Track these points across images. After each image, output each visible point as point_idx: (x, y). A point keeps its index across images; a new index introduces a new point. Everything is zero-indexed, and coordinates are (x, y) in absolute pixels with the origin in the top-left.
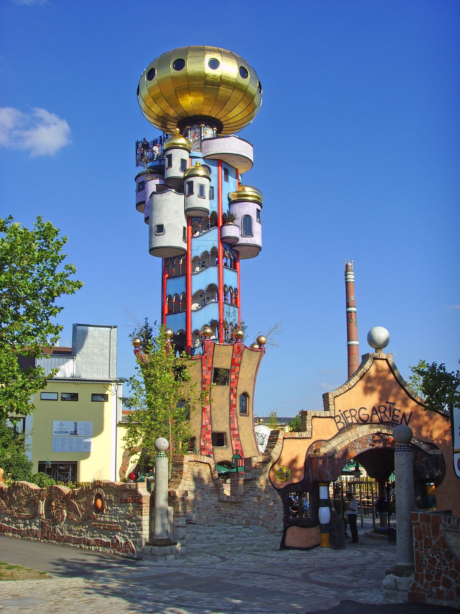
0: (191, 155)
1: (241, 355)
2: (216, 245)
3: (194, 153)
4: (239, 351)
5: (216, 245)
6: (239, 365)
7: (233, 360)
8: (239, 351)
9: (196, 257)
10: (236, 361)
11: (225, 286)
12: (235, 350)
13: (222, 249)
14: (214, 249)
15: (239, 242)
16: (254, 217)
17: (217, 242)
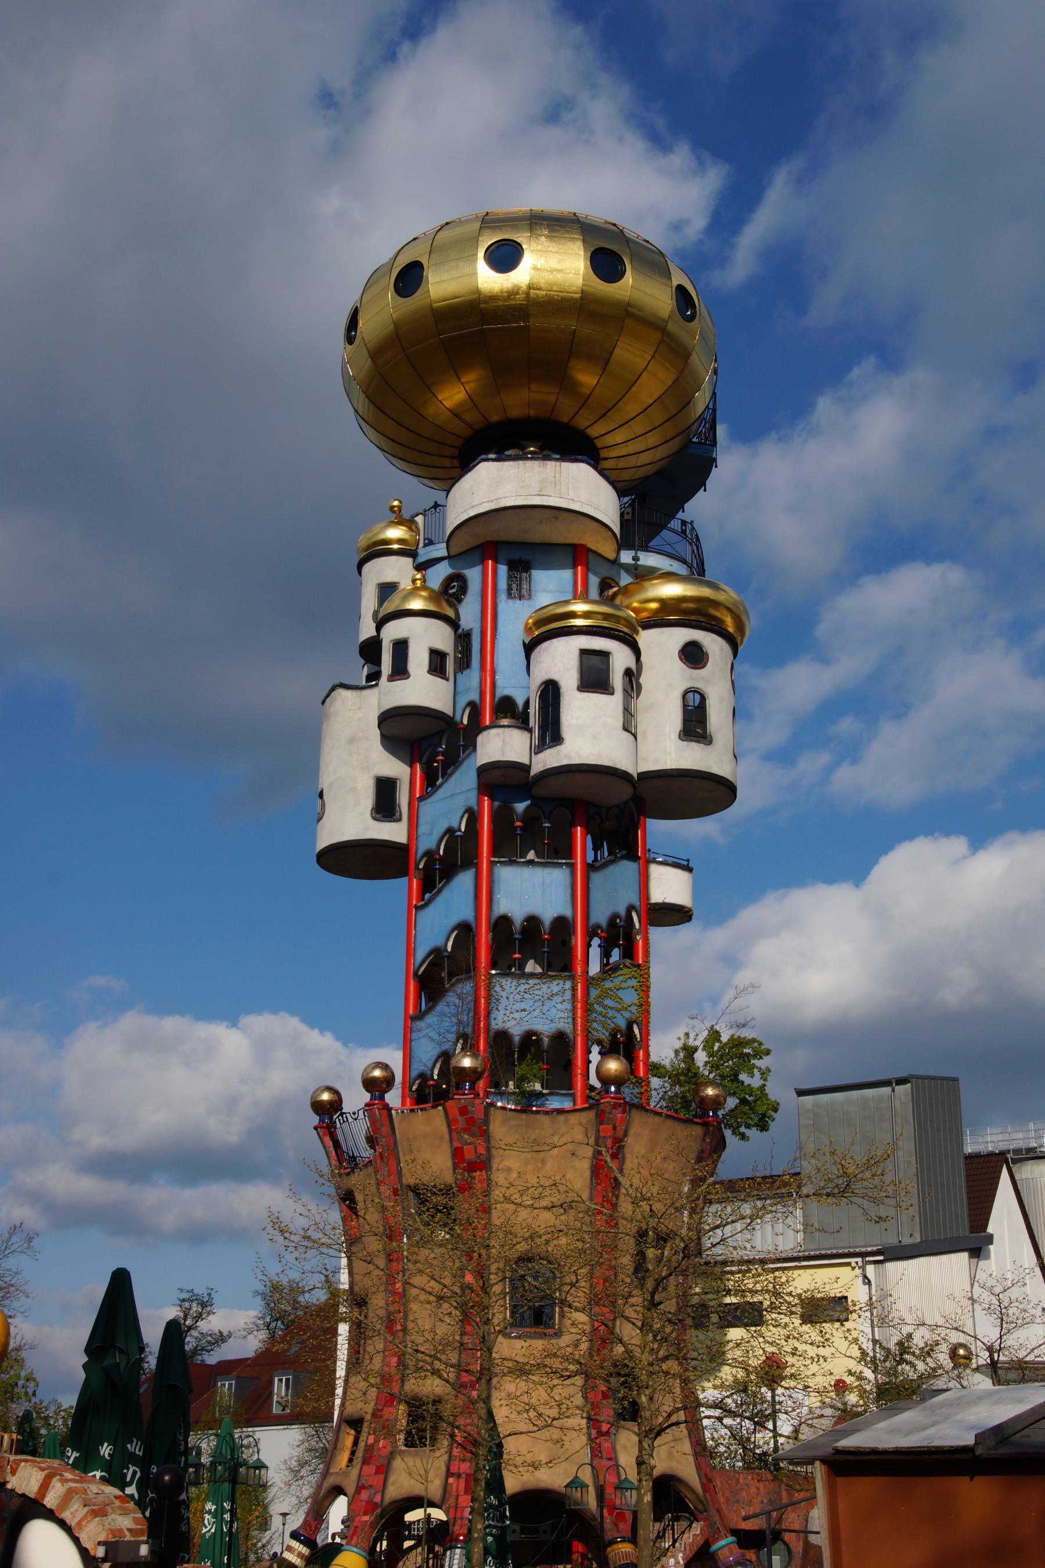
0: (421, 559)
1: (485, 1134)
2: (472, 799)
3: (425, 554)
4: (471, 1122)
5: (473, 802)
6: (483, 1164)
7: (457, 1154)
8: (471, 1122)
9: (429, 854)
10: (469, 1155)
11: (505, 920)
12: (456, 1121)
13: (491, 807)
14: (473, 816)
15: (533, 773)
16: (568, 679)
17: (475, 793)
